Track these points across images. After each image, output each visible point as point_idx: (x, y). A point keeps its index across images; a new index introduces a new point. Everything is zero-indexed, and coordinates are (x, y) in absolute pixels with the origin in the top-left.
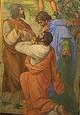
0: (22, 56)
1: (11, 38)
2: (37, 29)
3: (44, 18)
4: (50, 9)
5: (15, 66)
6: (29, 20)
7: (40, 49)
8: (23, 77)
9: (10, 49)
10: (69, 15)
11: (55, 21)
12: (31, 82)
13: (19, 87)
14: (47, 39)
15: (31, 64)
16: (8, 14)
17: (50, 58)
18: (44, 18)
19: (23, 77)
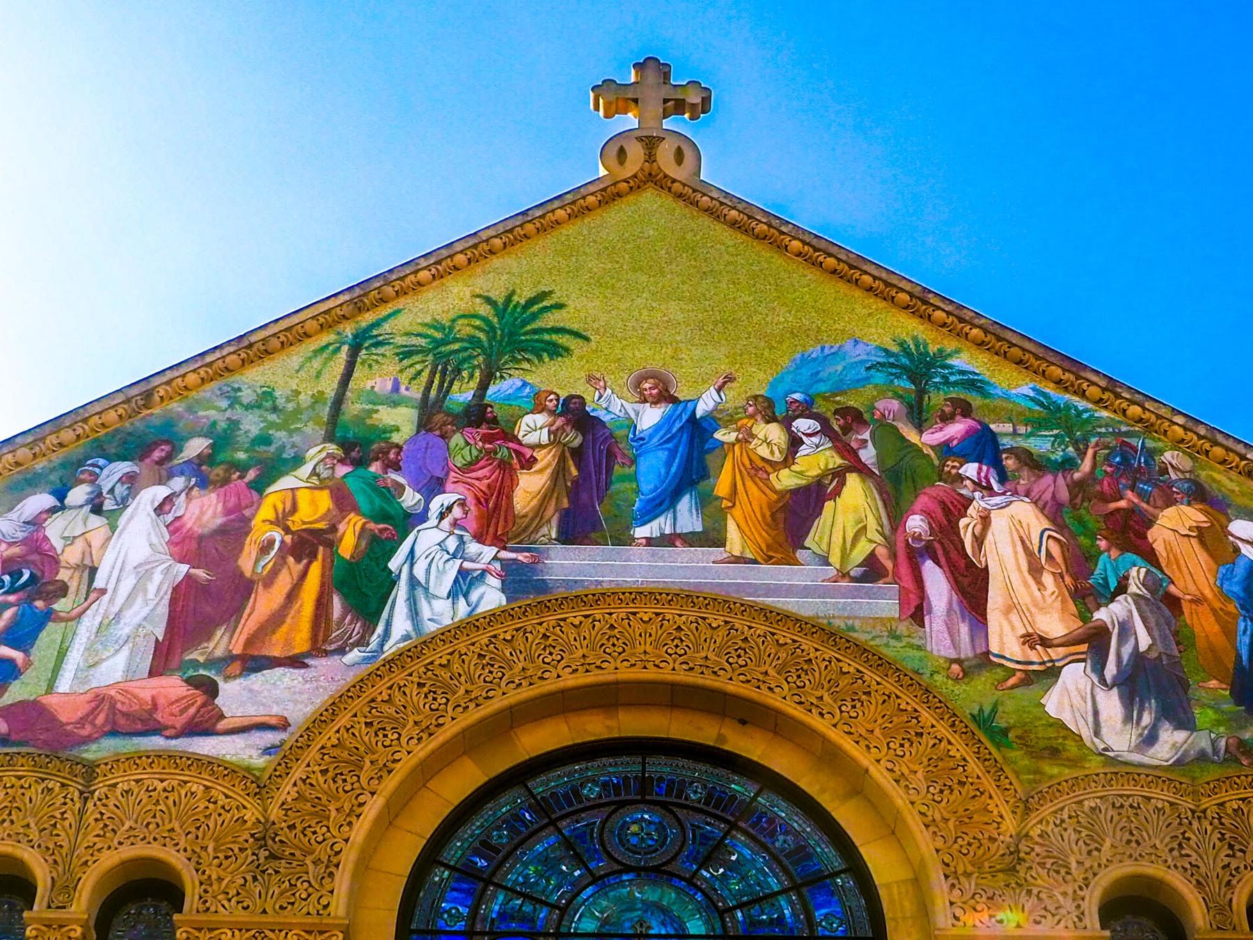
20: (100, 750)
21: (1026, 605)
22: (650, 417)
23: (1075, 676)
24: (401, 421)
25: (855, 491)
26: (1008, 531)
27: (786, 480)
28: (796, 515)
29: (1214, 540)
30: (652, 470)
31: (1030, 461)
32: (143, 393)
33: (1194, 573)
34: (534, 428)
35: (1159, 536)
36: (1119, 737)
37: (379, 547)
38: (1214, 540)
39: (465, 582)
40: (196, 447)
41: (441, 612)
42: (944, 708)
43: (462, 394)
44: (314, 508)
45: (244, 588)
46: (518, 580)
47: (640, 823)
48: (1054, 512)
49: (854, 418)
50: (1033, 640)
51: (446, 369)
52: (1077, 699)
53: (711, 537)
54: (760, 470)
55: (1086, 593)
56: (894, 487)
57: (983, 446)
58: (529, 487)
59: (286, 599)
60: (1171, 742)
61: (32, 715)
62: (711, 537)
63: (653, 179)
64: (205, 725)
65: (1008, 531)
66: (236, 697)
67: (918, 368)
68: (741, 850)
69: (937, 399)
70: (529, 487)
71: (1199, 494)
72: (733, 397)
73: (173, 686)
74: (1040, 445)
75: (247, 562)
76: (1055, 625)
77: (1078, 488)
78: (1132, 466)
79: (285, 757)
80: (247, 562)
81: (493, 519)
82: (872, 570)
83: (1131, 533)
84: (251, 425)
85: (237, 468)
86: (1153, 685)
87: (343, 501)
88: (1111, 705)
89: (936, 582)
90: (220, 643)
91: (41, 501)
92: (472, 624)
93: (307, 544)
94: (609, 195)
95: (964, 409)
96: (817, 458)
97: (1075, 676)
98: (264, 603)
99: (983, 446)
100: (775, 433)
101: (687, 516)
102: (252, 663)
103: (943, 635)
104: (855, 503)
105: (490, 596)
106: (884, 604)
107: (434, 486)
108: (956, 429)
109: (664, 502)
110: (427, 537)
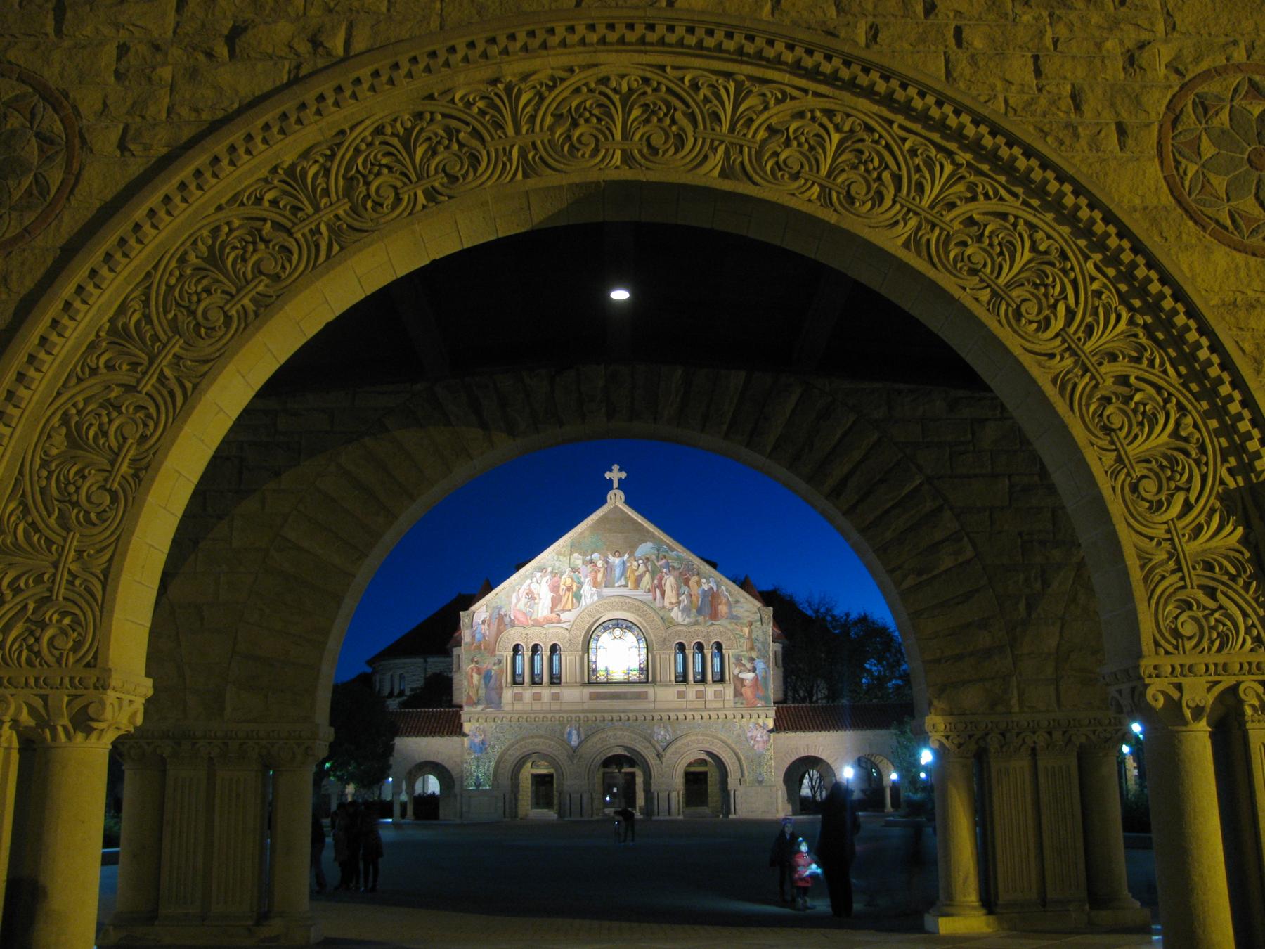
0: (742, 680)
1: (736, 671)
2: (749, 666)
4: (754, 655)
5: (739, 685)
7: (751, 675)
8: (743, 690)
9: (736, 677)
10: (764, 657)
12: (747, 692)
14: (754, 670)
15: (747, 683)
17: (756, 678)
18: (752, 660)
19: (743, 690)
21: (670, 596)
26: (670, 582)
27: (637, 573)
28: (638, 580)
30: (617, 572)
31: (674, 568)
33: (695, 590)
34: (600, 564)
36: (680, 620)
37: (579, 589)
38: (699, 584)
39: (592, 595)
41: (589, 601)
44: (569, 582)
45: (560, 598)
46: (600, 596)
48: (676, 578)
49: (648, 559)
52: (676, 614)
55: (679, 595)
58: (600, 575)
59: (567, 598)
60: (687, 619)
61: (536, 620)
62: (626, 586)
64: (559, 622)
74: (676, 565)
75: (561, 593)
76: (674, 601)
81: (595, 584)
82: (649, 591)
83: (687, 582)
86: (686, 610)
90: (560, 607)
91: (528, 581)
93: (569, 589)
96: (642, 568)
98: (564, 600)
99: (667, 565)
100: (635, 563)
102: (564, 611)
103: (658, 603)
104: (647, 576)
105: (595, 598)
106: (650, 597)
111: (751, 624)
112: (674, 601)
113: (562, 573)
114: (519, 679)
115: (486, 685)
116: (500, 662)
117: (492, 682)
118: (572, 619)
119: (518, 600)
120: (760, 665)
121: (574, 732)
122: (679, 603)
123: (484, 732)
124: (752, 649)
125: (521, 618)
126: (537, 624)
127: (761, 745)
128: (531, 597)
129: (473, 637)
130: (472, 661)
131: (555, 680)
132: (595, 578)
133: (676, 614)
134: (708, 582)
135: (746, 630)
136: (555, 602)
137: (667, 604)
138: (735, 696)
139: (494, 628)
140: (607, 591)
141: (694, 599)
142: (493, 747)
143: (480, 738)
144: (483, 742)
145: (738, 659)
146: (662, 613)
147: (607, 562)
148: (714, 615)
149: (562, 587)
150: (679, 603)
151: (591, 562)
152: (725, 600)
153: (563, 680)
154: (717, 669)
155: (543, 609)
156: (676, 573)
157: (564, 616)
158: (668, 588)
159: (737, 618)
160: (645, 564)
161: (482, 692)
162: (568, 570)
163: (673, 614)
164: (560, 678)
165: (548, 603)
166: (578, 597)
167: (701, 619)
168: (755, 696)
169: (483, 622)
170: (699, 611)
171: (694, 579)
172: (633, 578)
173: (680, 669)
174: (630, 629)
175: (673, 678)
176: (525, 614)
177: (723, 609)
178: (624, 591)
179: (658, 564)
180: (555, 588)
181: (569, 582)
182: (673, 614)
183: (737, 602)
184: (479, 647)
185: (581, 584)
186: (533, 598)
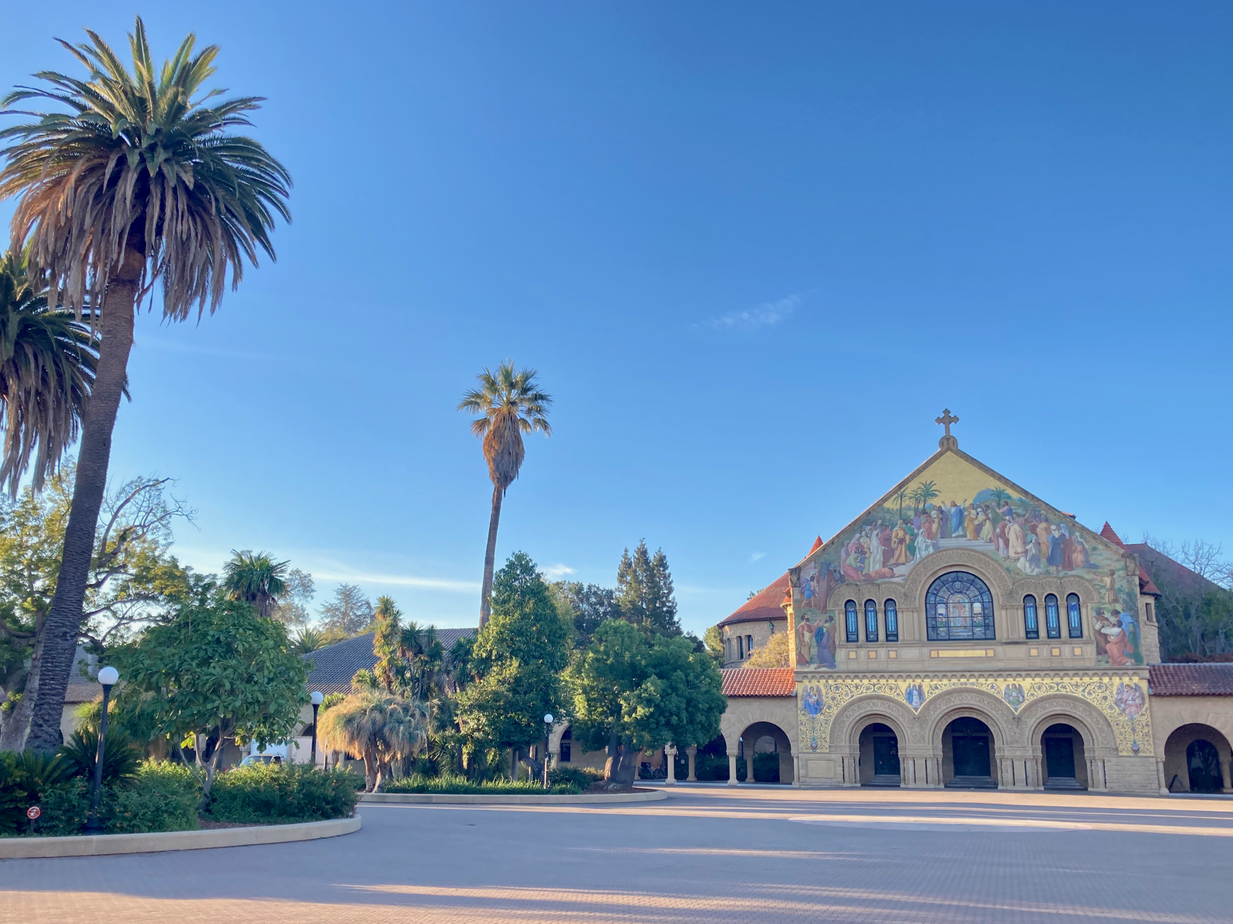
0: (1106, 636)
1: (1098, 627)
2: (1113, 620)
3: (1116, 613)
4: (1119, 607)
5: (1102, 643)
6: (1107, 615)
7: (1116, 630)
9: (1099, 632)
10: (1131, 609)
11: (1122, 613)
13: (1106, 652)
14: (1120, 624)
16: (1094, 614)
18: (1116, 613)
19: (1108, 647)
20: (879, 581)
21: (1016, 546)
22: (953, 510)
23: (1022, 559)
24: (911, 514)
25: (988, 525)
26: (1013, 531)
27: (976, 522)
28: (978, 529)
29: (1048, 530)
30: (954, 522)
31: (1018, 515)
32: (869, 512)
33: (1044, 538)
34: (934, 514)
35: (1038, 530)
36: (1028, 571)
37: (913, 540)
38: (1048, 530)
39: (927, 547)
40: (880, 522)
41: (924, 554)
42: (1002, 567)
43: (921, 506)
45: (893, 550)
46: (935, 546)
47: (958, 584)
48: (1021, 526)
49: (987, 507)
50: (1016, 553)
51: (918, 501)
52: (1023, 564)
53: (964, 536)
54: (972, 520)
55: (1025, 543)
56: (995, 522)
57: (1010, 512)
58: (935, 526)
62: (964, 536)
63: (949, 449)
64: (893, 576)
65: (1013, 531)
66: (896, 570)
67: (999, 494)
68: (972, 588)
69: (1002, 502)
70: (935, 526)
71: (1047, 520)
72: (967, 504)
73: (886, 570)
74: (1020, 511)
75: (893, 546)
76: (1019, 550)
77: (1026, 520)
78: (1037, 516)
79: (906, 580)
80: (893, 546)
81: (930, 535)
83: (1033, 530)
84: (888, 516)
85: (887, 526)
86: (1034, 560)
87: (905, 533)
88: (1028, 565)
89: (1001, 541)
90: (892, 561)
91: (858, 535)
92: (929, 556)
93: (901, 541)
94: (940, 454)
95: (1007, 503)
96: (981, 517)
97: (1022, 559)
98: (897, 553)
99: (1010, 512)
100: (974, 512)
101: (960, 532)
102: (897, 565)
103: (1002, 552)
104: (988, 525)
105: (931, 550)
106: (992, 547)
107: (919, 528)
108: (1006, 508)
109: (957, 529)
110: (920, 539)
111: (1112, 573)
112: (1019, 550)
113: (893, 526)
114: (853, 637)
115: (819, 642)
116: (831, 619)
117: (825, 640)
118: (906, 574)
119: (848, 555)
120: (1127, 619)
121: (915, 692)
122: (1026, 552)
123: (819, 690)
124: (1116, 601)
125: (851, 572)
126: (869, 580)
127: (1133, 709)
128: (862, 552)
129: (802, 593)
130: (803, 618)
131: (892, 637)
132: (930, 528)
133: (1023, 564)
134: (1059, 528)
135: (1108, 580)
136: (888, 554)
137: (1012, 554)
138: (1099, 653)
139: (824, 584)
140: (944, 543)
141: (1043, 547)
142: (829, 707)
143: (815, 698)
144: (818, 703)
145: (1099, 613)
146: (1007, 564)
147: (942, 512)
148: (1069, 565)
149: (894, 539)
150: (1026, 552)
151: (924, 512)
152: (1079, 548)
153: (900, 637)
154: (1075, 623)
155: (874, 565)
156: (1021, 520)
157: (896, 570)
158: (1012, 537)
159: (1095, 566)
160: (984, 512)
161: (814, 651)
162: (900, 522)
163: (1020, 564)
164: (897, 635)
165: (880, 557)
166: (912, 549)
167: (1052, 569)
168: (1123, 654)
169: (812, 579)
170: (1051, 560)
171: (1043, 525)
172: (971, 527)
173: (1032, 626)
174: (972, 583)
175: (1023, 634)
176: (856, 569)
177: (1078, 557)
178: (962, 542)
179: (999, 511)
180: (886, 541)
181: (901, 533)
182: (1020, 564)
183: (1094, 549)
184: (809, 604)
185: (914, 537)
186: (863, 553)
